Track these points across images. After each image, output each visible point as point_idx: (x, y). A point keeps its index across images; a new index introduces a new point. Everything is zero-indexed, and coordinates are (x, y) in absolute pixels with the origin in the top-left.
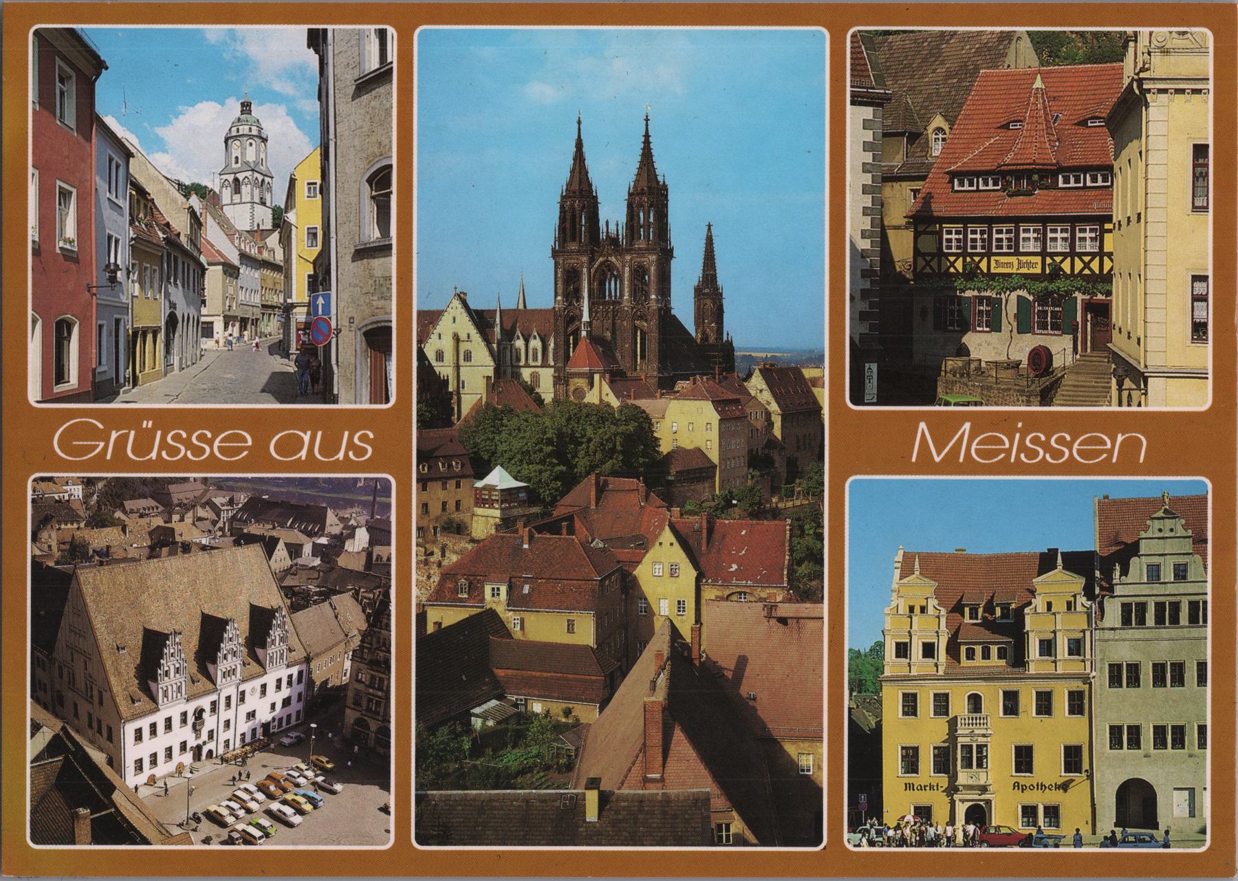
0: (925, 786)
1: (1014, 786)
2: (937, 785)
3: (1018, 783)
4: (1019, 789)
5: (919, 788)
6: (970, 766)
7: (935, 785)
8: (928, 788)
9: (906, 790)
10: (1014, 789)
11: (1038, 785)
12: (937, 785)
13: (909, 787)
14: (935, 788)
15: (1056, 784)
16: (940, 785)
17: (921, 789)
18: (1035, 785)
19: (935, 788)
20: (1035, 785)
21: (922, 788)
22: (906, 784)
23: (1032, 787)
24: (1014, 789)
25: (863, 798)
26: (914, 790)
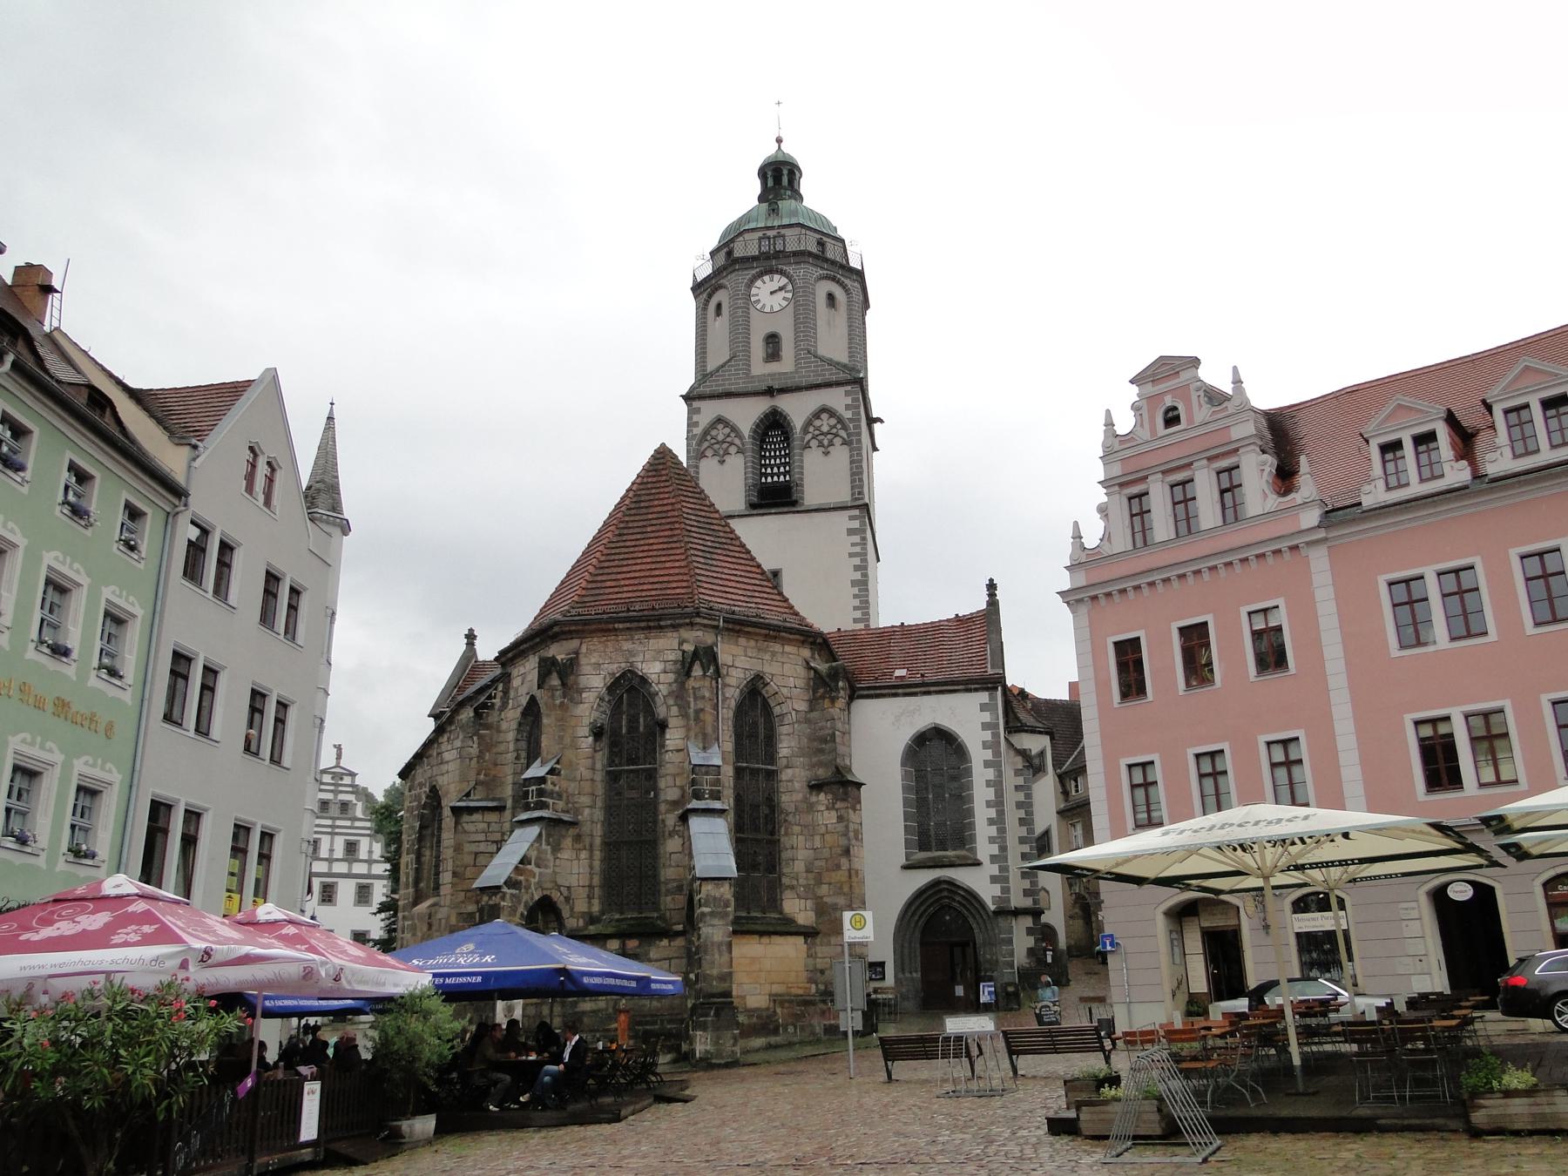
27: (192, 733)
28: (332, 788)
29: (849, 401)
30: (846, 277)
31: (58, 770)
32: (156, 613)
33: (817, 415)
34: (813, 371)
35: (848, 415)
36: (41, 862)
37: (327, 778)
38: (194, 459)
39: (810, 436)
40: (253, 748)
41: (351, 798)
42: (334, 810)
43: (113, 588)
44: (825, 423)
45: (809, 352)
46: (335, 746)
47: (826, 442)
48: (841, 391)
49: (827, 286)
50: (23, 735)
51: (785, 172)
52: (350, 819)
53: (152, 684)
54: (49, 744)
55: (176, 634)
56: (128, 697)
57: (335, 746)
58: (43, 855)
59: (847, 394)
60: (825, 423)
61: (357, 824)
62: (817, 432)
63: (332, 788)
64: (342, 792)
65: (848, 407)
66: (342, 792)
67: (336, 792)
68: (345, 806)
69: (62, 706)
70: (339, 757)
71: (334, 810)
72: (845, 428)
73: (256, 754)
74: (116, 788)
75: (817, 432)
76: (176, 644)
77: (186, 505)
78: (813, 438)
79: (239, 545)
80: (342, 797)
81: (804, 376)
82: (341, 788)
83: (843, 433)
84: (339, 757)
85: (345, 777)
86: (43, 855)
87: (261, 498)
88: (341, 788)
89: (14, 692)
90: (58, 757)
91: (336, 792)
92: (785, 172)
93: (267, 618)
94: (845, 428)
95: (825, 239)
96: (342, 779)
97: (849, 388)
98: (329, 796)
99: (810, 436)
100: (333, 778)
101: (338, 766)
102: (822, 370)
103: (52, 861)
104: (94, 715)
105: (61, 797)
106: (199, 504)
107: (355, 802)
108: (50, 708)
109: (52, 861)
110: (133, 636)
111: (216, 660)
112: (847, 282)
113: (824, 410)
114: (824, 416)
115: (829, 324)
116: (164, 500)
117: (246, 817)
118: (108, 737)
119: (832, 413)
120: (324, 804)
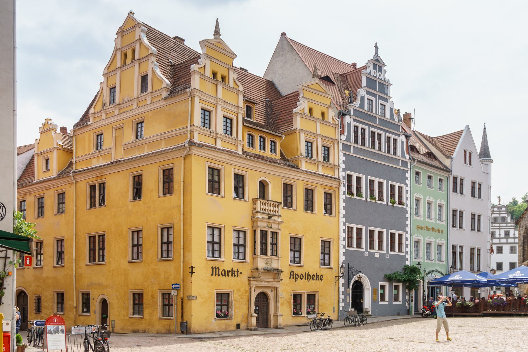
0: (228, 271)
1: (291, 275)
2: (238, 272)
3: (293, 272)
4: (293, 278)
5: (223, 273)
6: (264, 252)
7: (236, 271)
8: (230, 274)
9: (212, 275)
10: (290, 278)
11: (305, 275)
12: (238, 272)
13: (215, 271)
14: (236, 274)
15: (316, 274)
16: (240, 271)
17: (225, 276)
18: (304, 275)
19: (236, 274)
20: (304, 275)
21: (225, 274)
22: (212, 268)
23: (302, 277)
24: (290, 278)
25: (482, 285)
26: (219, 275)
27: (459, 229)
28: (498, 212)
31: (434, 242)
32: (448, 203)
36: (433, 262)
37: (496, 209)
38: (452, 162)
40: (473, 229)
41: (506, 215)
42: (499, 220)
43: (439, 200)
46: (498, 197)
50: (427, 237)
52: (505, 223)
53: (449, 219)
54: (432, 238)
55: (453, 206)
56: (445, 223)
57: (498, 197)
58: (434, 260)
61: (508, 225)
63: (498, 212)
64: (502, 214)
66: (502, 214)
67: (499, 214)
68: (503, 219)
69: (433, 229)
70: (500, 201)
71: (499, 220)
73: (474, 230)
74: (445, 243)
76: (453, 208)
77: (451, 174)
79: (464, 178)
80: (502, 215)
82: (501, 212)
84: (500, 201)
85: (502, 208)
86: (434, 260)
87: (468, 163)
88: (501, 212)
89: (425, 229)
90: (434, 240)
91: (499, 214)
93: (473, 195)
96: (501, 209)
98: (497, 215)
100: (498, 209)
101: (499, 204)
103: (435, 261)
104: (439, 229)
105: (435, 248)
106: (455, 173)
107: (507, 217)
108: (431, 230)
109: (435, 261)
110: (444, 208)
111: (462, 209)
116: (446, 174)
117: (473, 246)
118: (442, 233)
120: (496, 219)
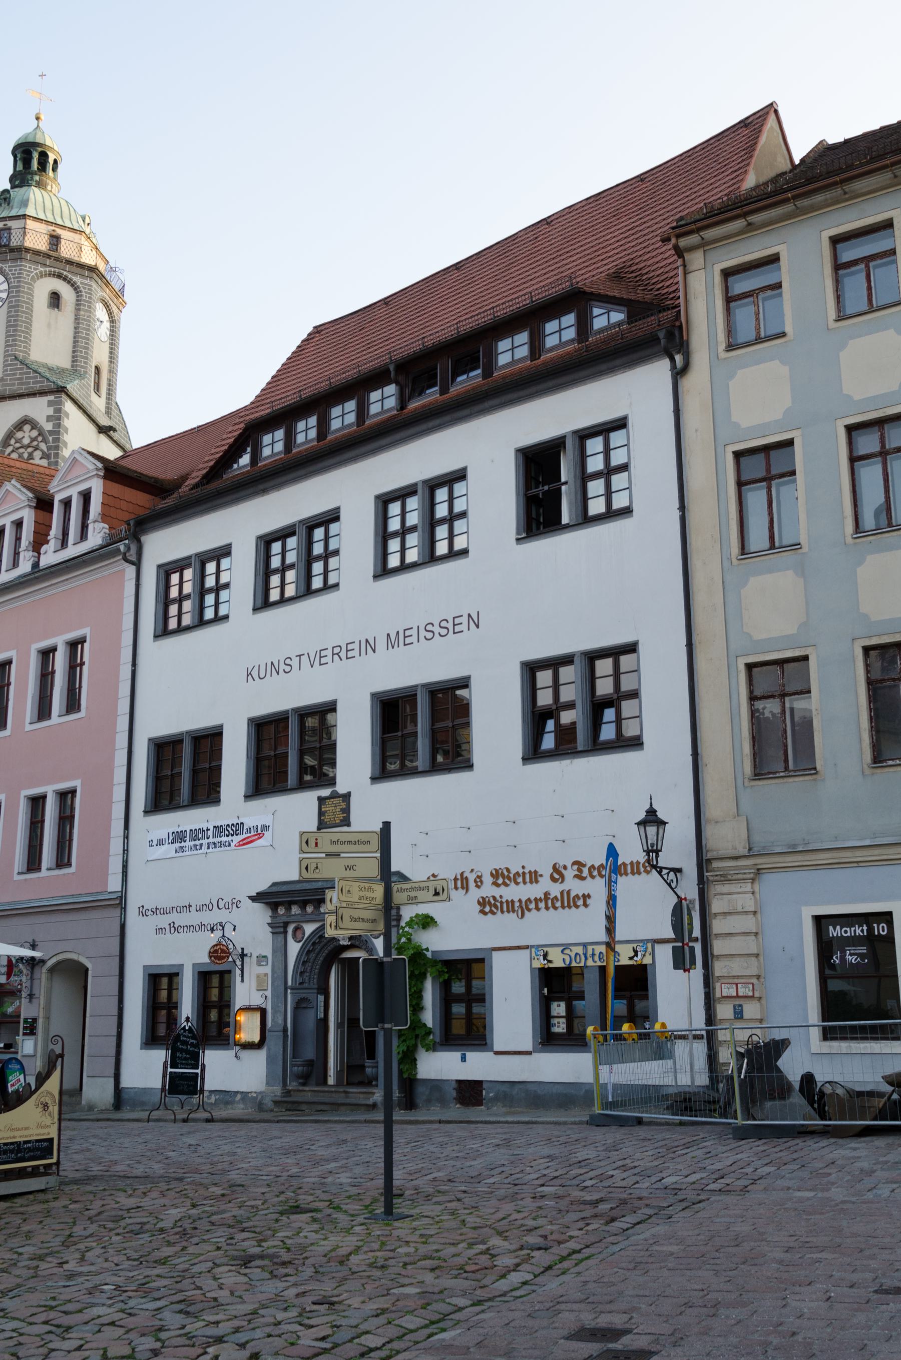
29: (50, 411)
30: (76, 274)
33: (19, 426)
34: (19, 379)
35: (48, 427)
39: (10, 449)
44: (26, 435)
45: (16, 358)
47: (26, 456)
48: (43, 401)
49: (44, 287)
51: (36, 156)
59: (50, 404)
60: (26, 435)
62: (18, 445)
65: (49, 418)
72: (45, 440)
75: (18, 445)
78: (13, 451)
81: (8, 385)
83: (43, 446)
92: (36, 156)
94: (45, 440)
95: (59, 231)
97: (52, 398)
99: (10, 449)
102: (26, 378)
112: (77, 279)
113: (25, 422)
114: (27, 428)
115: (49, 325)
119: (34, 425)
